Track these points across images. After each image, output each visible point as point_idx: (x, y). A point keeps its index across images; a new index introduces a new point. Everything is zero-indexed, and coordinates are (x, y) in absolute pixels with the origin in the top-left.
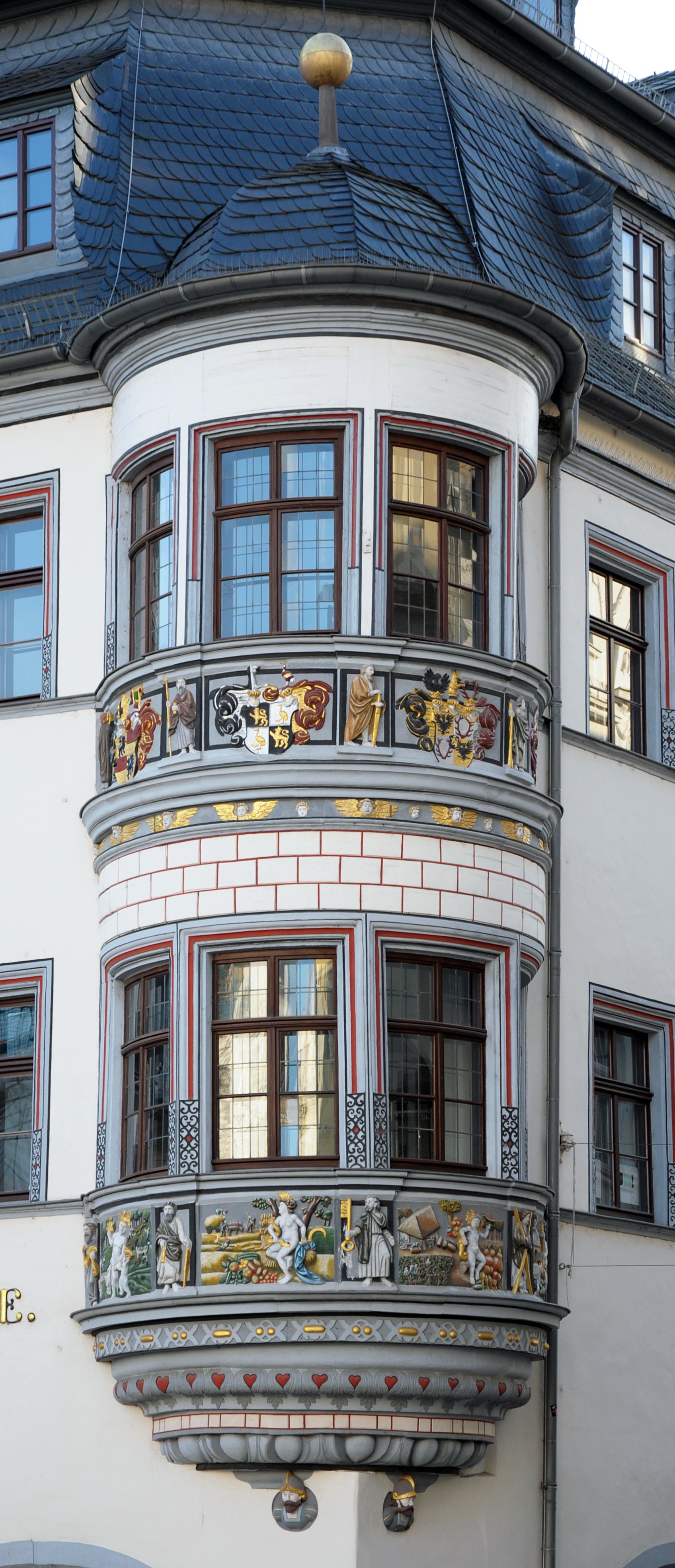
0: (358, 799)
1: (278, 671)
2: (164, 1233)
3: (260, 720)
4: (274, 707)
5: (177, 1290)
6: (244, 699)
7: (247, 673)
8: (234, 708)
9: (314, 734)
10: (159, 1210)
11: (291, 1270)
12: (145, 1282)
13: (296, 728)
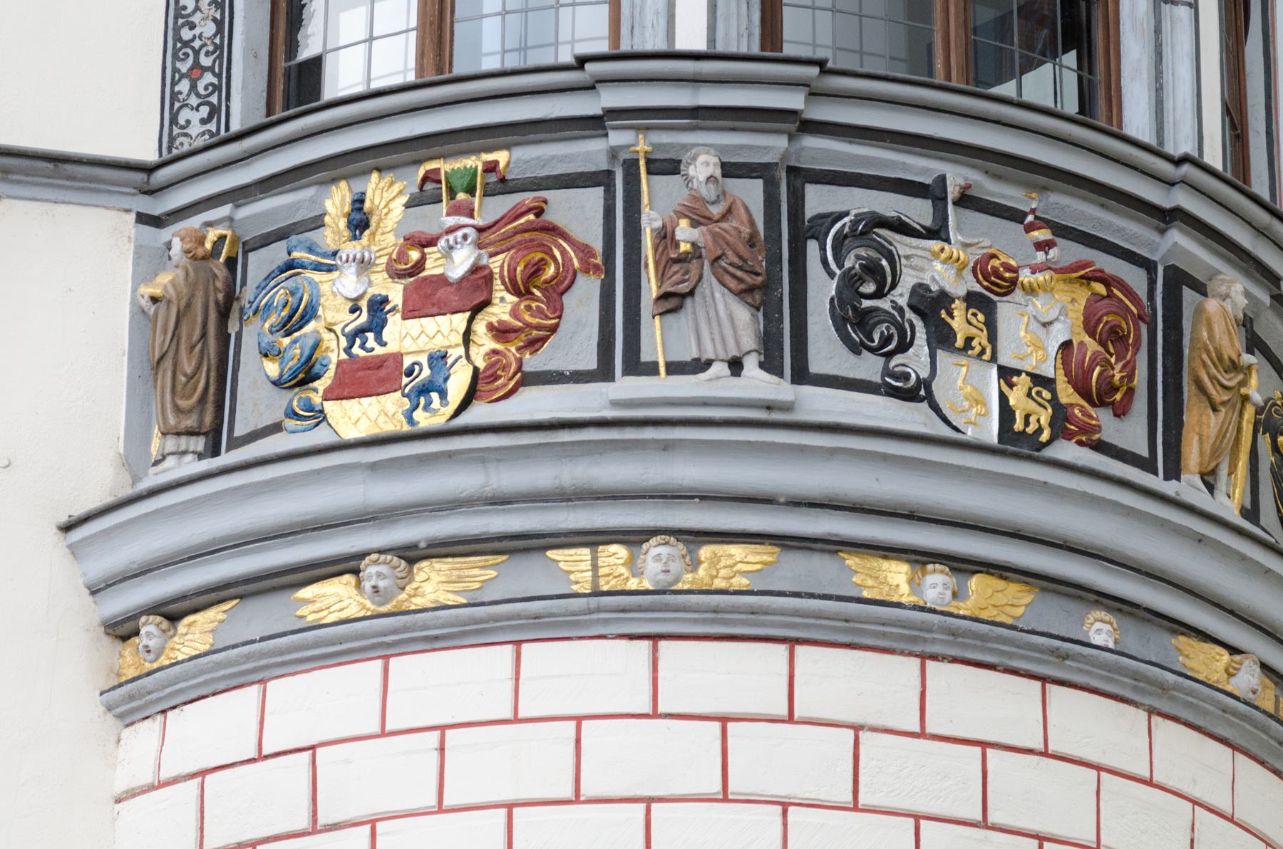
0: (1234, 650)
1: (1015, 216)
3: (969, 340)
4: (1006, 310)
6: (930, 267)
7: (933, 192)
8: (893, 286)
9: (1111, 428)
13: (1067, 394)
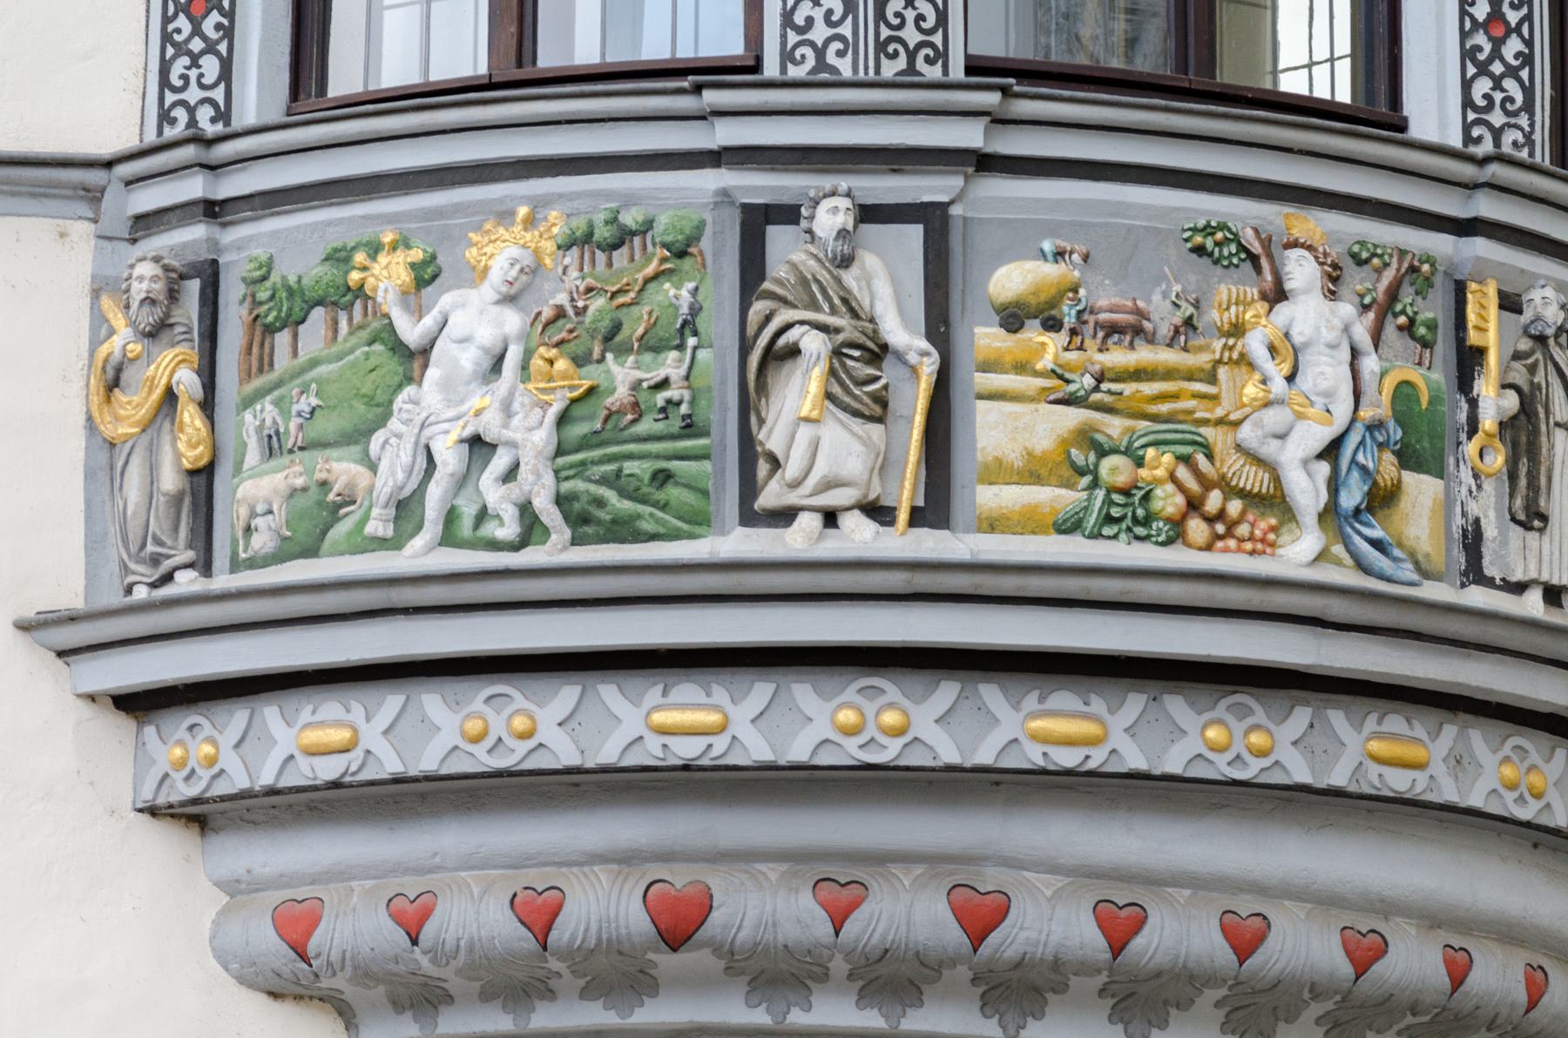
2: (815, 306)
5: (860, 536)
10: (758, 220)
11: (1330, 514)
12: (673, 493)
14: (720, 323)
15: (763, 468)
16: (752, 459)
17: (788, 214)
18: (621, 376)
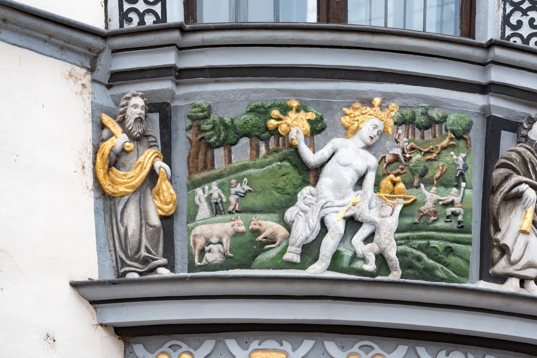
12: (452, 259)
14: (475, 177)
15: (496, 253)
16: (491, 248)
17: (514, 126)
18: (430, 196)
